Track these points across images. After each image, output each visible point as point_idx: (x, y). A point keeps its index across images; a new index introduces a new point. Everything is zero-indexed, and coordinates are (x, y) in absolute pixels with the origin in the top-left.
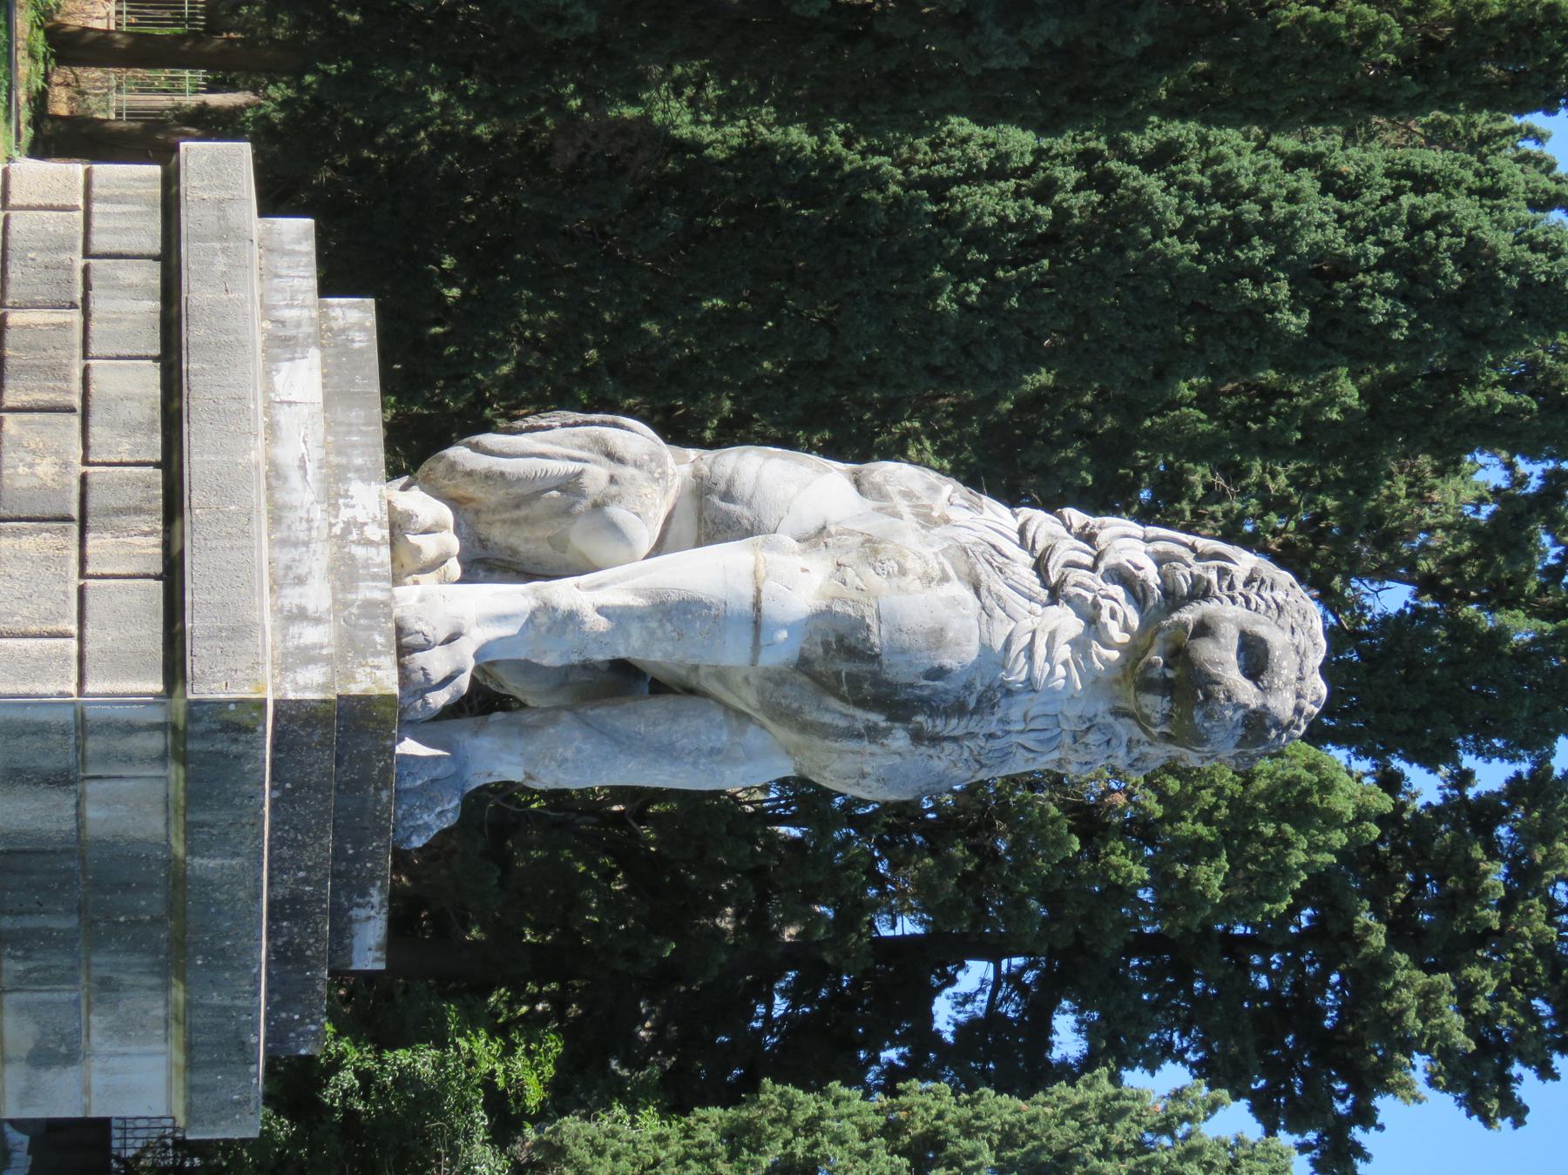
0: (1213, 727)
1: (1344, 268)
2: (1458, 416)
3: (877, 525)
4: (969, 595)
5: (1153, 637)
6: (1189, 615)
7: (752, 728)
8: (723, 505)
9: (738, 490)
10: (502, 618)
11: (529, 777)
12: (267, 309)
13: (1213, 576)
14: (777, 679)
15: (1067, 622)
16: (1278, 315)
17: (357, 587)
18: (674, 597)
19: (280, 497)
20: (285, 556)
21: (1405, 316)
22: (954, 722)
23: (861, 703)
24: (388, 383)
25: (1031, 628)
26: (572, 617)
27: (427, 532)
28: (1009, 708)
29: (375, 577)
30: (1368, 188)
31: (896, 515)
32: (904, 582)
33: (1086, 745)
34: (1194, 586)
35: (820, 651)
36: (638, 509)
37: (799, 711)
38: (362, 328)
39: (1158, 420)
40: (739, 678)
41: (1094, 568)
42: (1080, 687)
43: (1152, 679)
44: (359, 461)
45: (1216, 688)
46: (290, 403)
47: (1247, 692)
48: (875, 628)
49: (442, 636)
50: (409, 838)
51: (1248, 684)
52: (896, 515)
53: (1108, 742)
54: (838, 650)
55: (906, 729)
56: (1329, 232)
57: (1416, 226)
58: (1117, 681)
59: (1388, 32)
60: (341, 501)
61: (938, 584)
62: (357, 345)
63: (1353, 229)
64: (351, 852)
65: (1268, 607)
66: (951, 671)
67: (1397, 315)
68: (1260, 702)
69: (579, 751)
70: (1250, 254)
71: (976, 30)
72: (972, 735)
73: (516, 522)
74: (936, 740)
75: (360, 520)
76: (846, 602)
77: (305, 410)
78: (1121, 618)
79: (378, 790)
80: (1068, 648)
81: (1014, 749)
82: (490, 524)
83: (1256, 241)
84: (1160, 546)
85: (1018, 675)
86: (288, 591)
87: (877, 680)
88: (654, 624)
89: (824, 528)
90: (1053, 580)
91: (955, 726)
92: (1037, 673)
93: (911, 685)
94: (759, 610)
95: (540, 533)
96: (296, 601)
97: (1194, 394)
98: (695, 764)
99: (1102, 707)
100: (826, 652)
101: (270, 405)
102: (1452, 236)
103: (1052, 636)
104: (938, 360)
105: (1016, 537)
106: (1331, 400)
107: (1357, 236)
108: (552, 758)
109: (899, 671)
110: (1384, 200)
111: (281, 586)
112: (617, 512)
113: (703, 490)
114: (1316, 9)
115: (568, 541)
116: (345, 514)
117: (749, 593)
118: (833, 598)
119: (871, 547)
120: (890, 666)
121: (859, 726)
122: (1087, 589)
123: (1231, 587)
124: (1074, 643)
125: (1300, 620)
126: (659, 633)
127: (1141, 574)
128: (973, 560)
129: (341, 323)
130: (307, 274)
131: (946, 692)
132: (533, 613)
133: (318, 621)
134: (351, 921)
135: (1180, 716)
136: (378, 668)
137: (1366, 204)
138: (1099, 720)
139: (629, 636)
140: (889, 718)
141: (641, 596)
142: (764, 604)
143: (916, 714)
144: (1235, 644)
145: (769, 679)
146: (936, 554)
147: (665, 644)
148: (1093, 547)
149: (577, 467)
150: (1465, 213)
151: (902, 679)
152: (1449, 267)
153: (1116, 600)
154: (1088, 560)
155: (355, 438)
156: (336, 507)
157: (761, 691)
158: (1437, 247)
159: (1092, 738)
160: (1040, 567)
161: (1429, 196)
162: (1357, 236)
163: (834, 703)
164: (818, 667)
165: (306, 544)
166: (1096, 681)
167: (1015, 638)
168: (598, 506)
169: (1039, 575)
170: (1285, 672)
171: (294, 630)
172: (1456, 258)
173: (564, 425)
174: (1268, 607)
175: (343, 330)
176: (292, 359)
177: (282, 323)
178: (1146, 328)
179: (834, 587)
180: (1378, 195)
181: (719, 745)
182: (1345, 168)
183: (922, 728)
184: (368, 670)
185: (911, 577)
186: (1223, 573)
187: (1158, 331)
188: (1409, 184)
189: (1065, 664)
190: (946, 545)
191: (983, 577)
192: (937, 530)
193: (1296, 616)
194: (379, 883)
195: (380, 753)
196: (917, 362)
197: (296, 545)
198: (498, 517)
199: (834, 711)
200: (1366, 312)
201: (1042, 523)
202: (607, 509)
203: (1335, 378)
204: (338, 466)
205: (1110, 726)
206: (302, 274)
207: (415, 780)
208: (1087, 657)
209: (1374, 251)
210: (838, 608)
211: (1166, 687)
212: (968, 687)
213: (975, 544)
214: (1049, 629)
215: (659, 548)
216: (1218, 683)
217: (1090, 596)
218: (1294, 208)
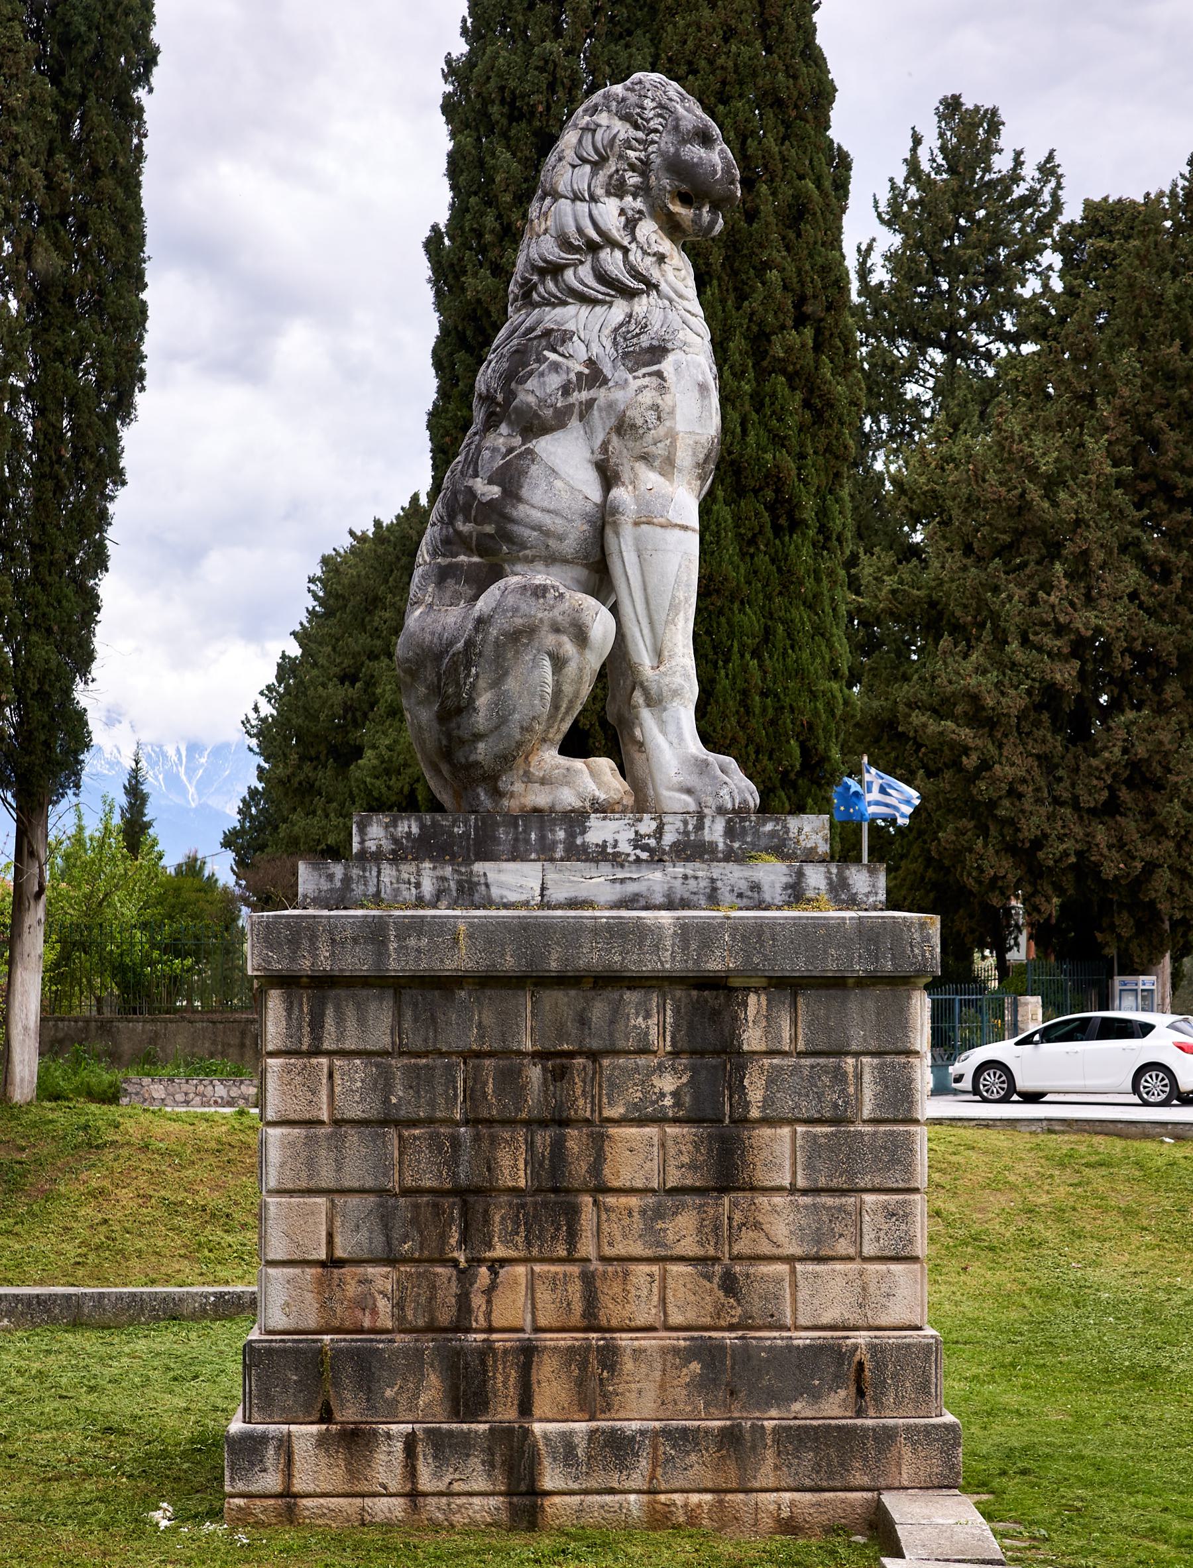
12: (420, 902)
17: (711, 843)
19: (659, 899)
20: (726, 896)
31: (590, 403)
44: (561, 835)
46: (543, 889)
52: (590, 403)
60: (610, 850)
62: (415, 830)
75: (632, 836)
77: (551, 876)
86: (767, 897)
96: (779, 891)
101: (545, 905)
105: (599, 309)
111: (761, 902)
116: (625, 847)
130: (375, 870)
133: (800, 874)
136: (800, 830)
155: (533, 836)
156: (617, 855)
165: (713, 880)
171: (810, 894)
175: (395, 841)
176: (487, 885)
177: (439, 894)
184: (802, 837)
185: (660, 402)
197: (715, 889)
204: (566, 850)
206: (374, 873)
213: (615, 343)
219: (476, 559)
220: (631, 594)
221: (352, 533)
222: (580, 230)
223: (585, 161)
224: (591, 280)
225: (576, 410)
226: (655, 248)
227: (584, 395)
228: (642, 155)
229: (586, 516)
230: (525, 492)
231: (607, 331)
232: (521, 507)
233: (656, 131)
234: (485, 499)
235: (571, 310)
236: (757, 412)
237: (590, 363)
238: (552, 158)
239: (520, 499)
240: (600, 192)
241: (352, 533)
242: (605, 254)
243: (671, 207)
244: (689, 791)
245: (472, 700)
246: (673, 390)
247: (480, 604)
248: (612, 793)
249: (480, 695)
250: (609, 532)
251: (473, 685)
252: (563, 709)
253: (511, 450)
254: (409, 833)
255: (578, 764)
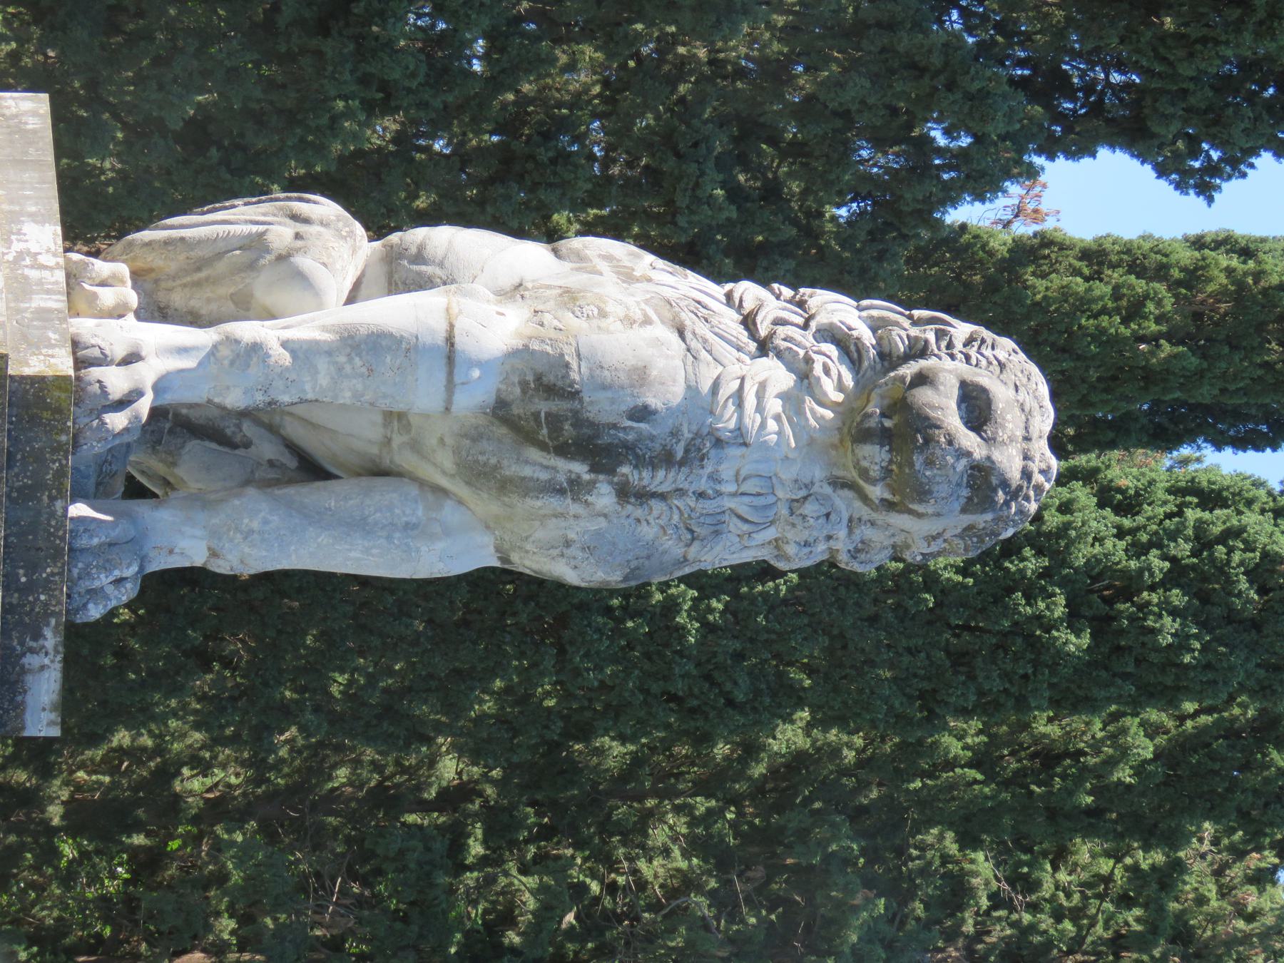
0: (934, 476)
1: (1129, 586)
2: (1267, 781)
3: (576, 280)
4: (674, 338)
5: (869, 395)
6: (908, 370)
7: (449, 506)
8: (415, 267)
9: (429, 252)
10: (183, 351)
11: (214, 554)
13: (931, 337)
14: (476, 436)
15: (779, 377)
16: (1055, 633)
18: (363, 331)
21: (1196, 637)
22: (661, 474)
23: (562, 450)
24: (60, 150)
25: (740, 374)
26: (256, 348)
27: (103, 284)
28: (719, 462)
29: (48, 292)
30: (1149, 504)
32: (604, 323)
33: (804, 517)
34: (910, 347)
35: (518, 391)
36: (325, 260)
37: (497, 467)
38: (34, 113)
39: (929, 782)
40: (434, 441)
41: (805, 327)
42: (793, 445)
43: (869, 428)
45: (937, 432)
47: (969, 440)
48: (574, 365)
49: (120, 353)
50: (85, 605)
51: (972, 435)
53: (828, 515)
54: (536, 389)
55: (611, 483)
56: (1109, 544)
57: (1203, 541)
58: (834, 447)
59: (1159, 303)
60: (13, 237)
63: (1134, 544)
64: (23, 579)
65: (990, 363)
66: (655, 412)
67: (1188, 637)
68: (984, 453)
69: (266, 522)
70: (1021, 566)
71: (705, 261)
72: (681, 492)
73: (198, 284)
74: (643, 496)
76: (543, 341)
78: (835, 377)
79: (52, 499)
80: (779, 402)
81: (726, 517)
82: (170, 290)
83: (1027, 552)
84: (875, 313)
85: (728, 421)
87: (578, 420)
88: (342, 359)
89: (521, 285)
90: (763, 331)
91: (661, 480)
92: (747, 421)
93: (614, 426)
94: (452, 345)
95: (225, 290)
97: (969, 754)
98: (389, 538)
99: (818, 473)
100: (524, 392)
102: (1244, 551)
103: (762, 387)
104: (679, 687)
105: (724, 299)
106: (1124, 752)
107: (1138, 550)
108: (237, 529)
109: (600, 408)
110: (1169, 516)
112: (304, 262)
113: (392, 258)
114: (1079, 279)
115: (252, 295)
116: (17, 246)
117: (441, 328)
118: (530, 338)
119: (570, 298)
120: (592, 403)
121: (562, 478)
122: (798, 345)
123: (950, 345)
124: (784, 396)
125: (1025, 380)
126: (348, 368)
127: (855, 333)
129: (14, 110)
131: (652, 438)
132: (215, 347)
134: (24, 671)
135: (900, 466)
136: (53, 356)
137: (1149, 519)
138: (816, 489)
139: (317, 372)
140: (593, 469)
141: (328, 331)
142: (458, 340)
143: (621, 464)
144: (955, 393)
145: (466, 436)
146: (638, 303)
147: (354, 381)
148: (805, 311)
149: (261, 228)
150: (1258, 528)
151: (605, 418)
152: (1243, 585)
153: (829, 357)
154: (800, 321)
157: (456, 451)
158: (1229, 562)
159: (810, 508)
160: (749, 322)
161: (1217, 512)
162: (1138, 550)
163: (534, 454)
164: (516, 410)
166: (812, 442)
167: (723, 382)
168: (283, 258)
169: (747, 328)
170: (1010, 426)
172: (1251, 574)
173: (246, 204)
174: (990, 363)
175: (16, 116)
178: (909, 650)
179: (532, 329)
180: (1161, 511)
181: (414, 520)
182: (1123, 482)
183: (627, 482)
185: (611, 319)
186: (940, 335)
187: (923, 655)
188: (1196, 500)
189: (777, 418)
191: (688, 323)
192: (638, 285)
193: (1020, 375)
194: (53, 621)
195: (55, 450)
196: (655, 688)
198: (178, 282)
199: (534, 464)
200: (1153, 631)
201: (748, 291)
202: (292, 259)
203: (1124, 731)
204: (10, 212)
205: (827, 498)
207: (91, 537)
208: (799, 411)
209: (1158, 565)
210: (535, 346)
211: (885, 437)
212: (675, 434)
214: (760, 378)
215: (351, 300)
216: (939, 427)
217: (802, 352)
218: (1068, 518)
254: (26, 123)
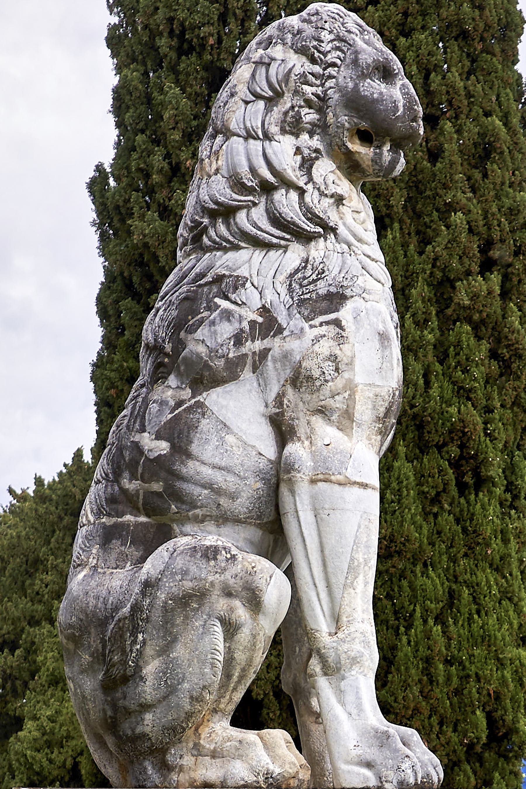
31: (264, 354)
52: (264, 354)
61: (344, 330)
128: (314, 296)
146: (311, 327)
185: (338, 352)
190: (298, 316)
213: (290, 290)
219: (143, 519)
220: (307, 556)
221: (11, 491)
222: (253, 170)
223: (258, 97)
224: (265, 224)
225: (249, 361)
226: (332, 189)
227: (258, 345)
228: (319, 91)
229: (259, 474)
230: (194, 448)
231: (281, 277)
232: (191, 464)
233: (334, 65)
234: (153, 455)
235: (244, 254)
236: (441, 363)
237: (264, 311)
238: (223, 94)
239: (189, 455)
240: (274, 129)
241: (11, 491)
242: (279, 196)
243: (350, 145)
244: (369, 765)
245: (138, 668)
246: (351, 340)
247: (147, 566)
248: (287, 767)
249: (147, 663)
250: (284, 490)
251: (140, 653)
252: (235, 678)
253: (180, 403)
255: (251, 736)
